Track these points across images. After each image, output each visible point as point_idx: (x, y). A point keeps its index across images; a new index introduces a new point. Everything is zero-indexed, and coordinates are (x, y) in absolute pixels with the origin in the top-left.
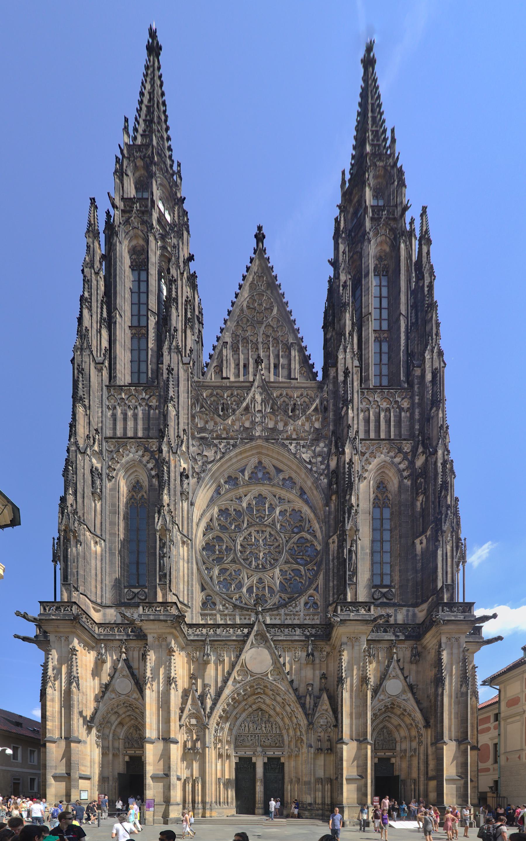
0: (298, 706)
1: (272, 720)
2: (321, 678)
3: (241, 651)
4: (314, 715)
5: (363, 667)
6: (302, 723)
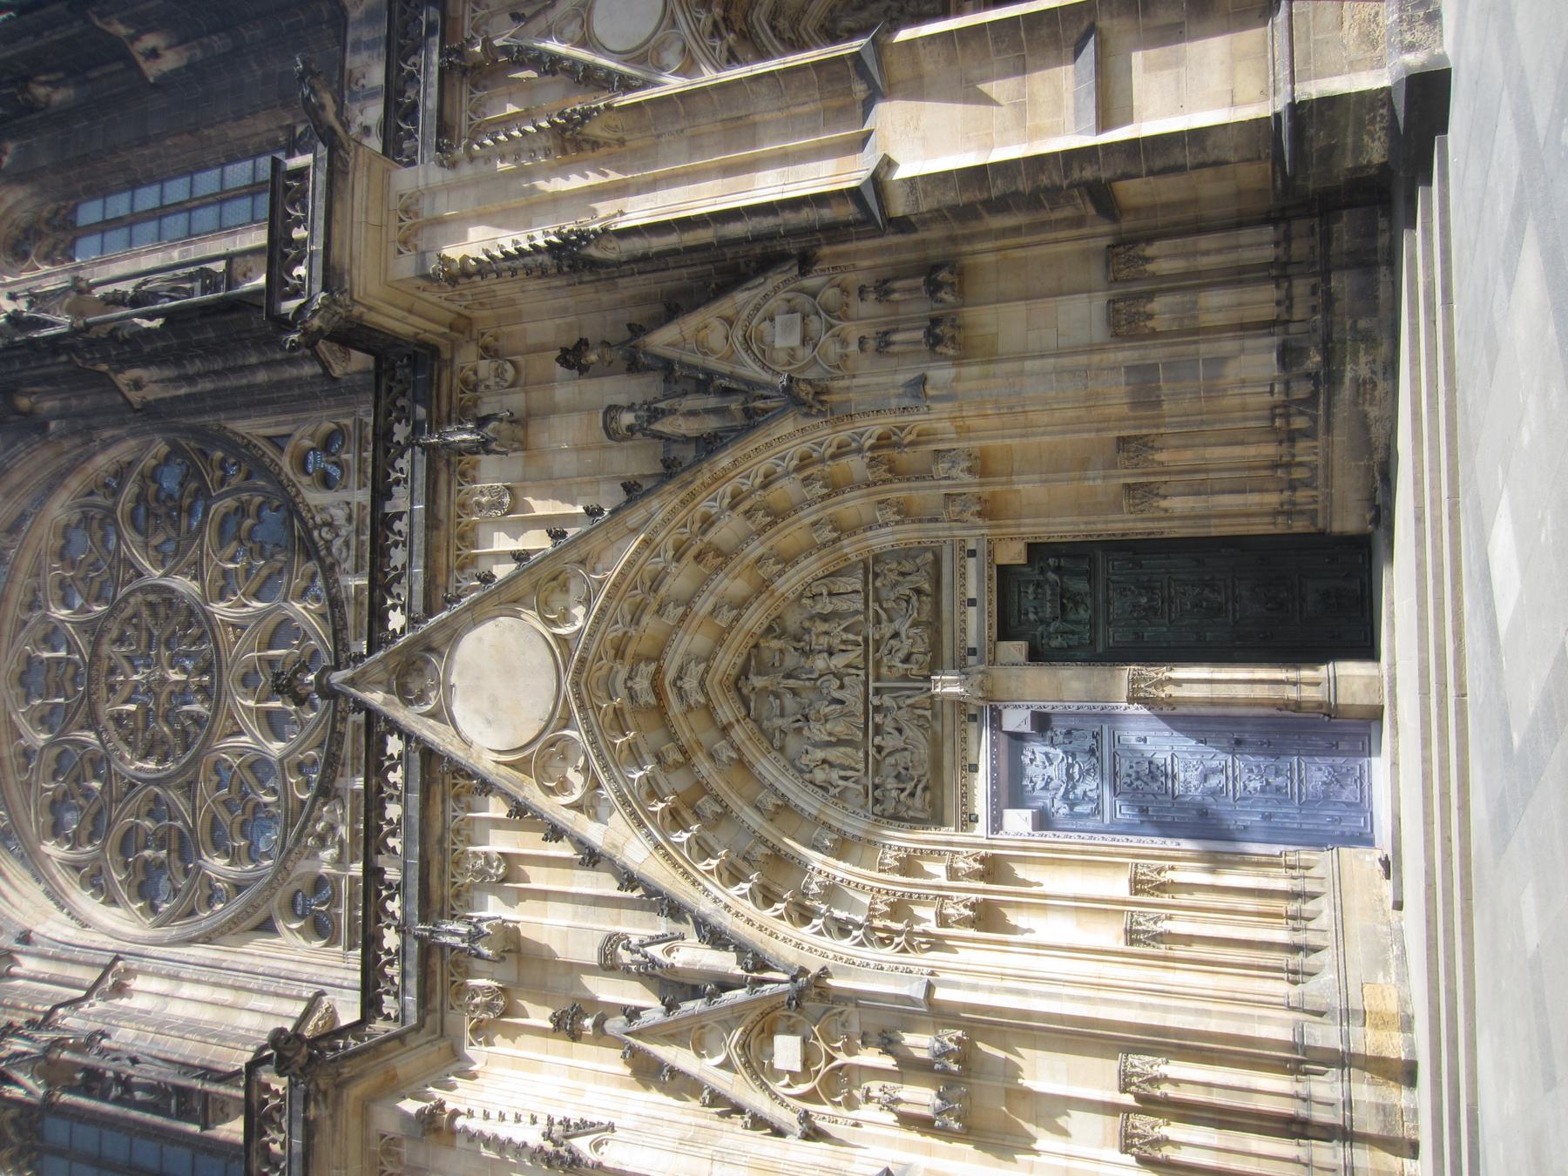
0: (705, 476)
1: (793, 621)
2: (583, 370)
3: (460, 771)
4: (751, 388)
5: (517, 156)
6: (796, 447)
